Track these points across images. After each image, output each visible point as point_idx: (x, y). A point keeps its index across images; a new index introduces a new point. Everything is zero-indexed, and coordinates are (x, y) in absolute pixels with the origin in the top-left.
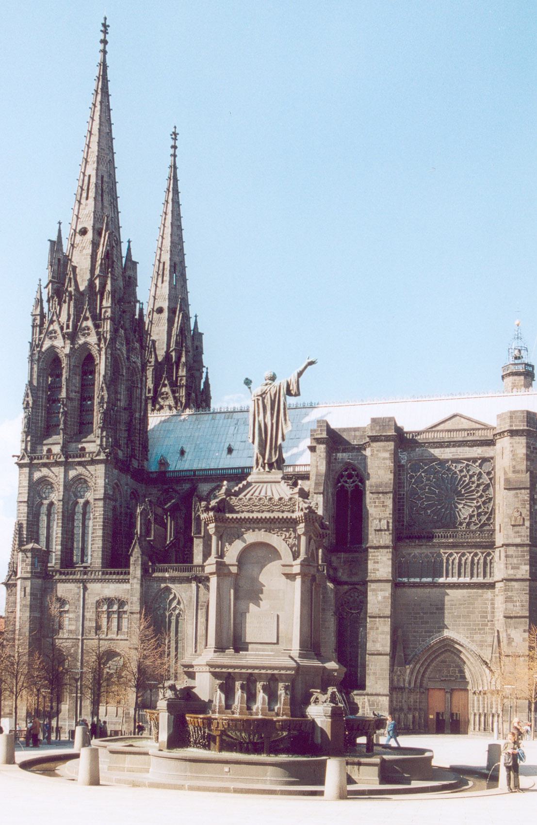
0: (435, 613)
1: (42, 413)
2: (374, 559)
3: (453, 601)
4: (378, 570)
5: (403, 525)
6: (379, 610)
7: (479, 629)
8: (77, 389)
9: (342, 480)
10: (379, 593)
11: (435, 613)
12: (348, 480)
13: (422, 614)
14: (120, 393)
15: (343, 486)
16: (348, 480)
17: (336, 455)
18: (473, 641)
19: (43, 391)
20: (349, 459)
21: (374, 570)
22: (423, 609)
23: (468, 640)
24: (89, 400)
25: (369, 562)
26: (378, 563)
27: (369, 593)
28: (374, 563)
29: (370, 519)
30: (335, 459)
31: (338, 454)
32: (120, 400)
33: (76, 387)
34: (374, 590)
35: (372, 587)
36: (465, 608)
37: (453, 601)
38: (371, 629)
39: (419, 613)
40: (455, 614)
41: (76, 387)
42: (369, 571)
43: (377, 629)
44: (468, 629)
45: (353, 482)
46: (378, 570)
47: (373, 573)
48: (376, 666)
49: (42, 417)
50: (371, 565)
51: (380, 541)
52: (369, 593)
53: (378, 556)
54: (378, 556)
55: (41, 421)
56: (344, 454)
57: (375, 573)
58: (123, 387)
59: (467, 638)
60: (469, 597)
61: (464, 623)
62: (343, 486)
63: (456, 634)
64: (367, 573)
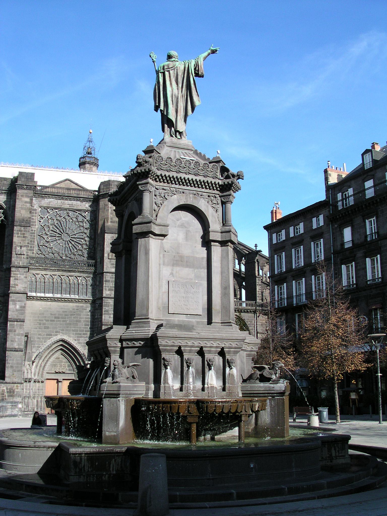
0: (54, 321)
2: (15, 277)
3: (66, 312)
4: (17, 285)
5: (33, 253)
6: (17, 316)
7: (84, 334)
10: (18, 303)
11: (54, 321)
13: (44, 321)
18: (79, 343)
21: (14, 284)
22: (46, 317)
23: (76, 342)
25: (11, 278)
26: (17, 279)
27: (10, 302)
28: (15, 279)
29: (14, 246)
34: (13, 301)
35: (12, 298)
36: (74, 318)
37: (66, 312)
38: (11, 331)
39: (43, 320)
40: (68, 322)
42: (11, 286)
43: (15, 331)
44: (76, 334)
46: (17, 285)
47: (14, 287)
48: (13, 360)
50: (12, 282)
51: (20, 263)
52: (10, 303)
53: (18, 274)
54: (18, 274)
57: (15, 287)
59: (75, 340)
60: (77, 310)
61: (74, 329)
63: (68, 337)
64: (9, 287)
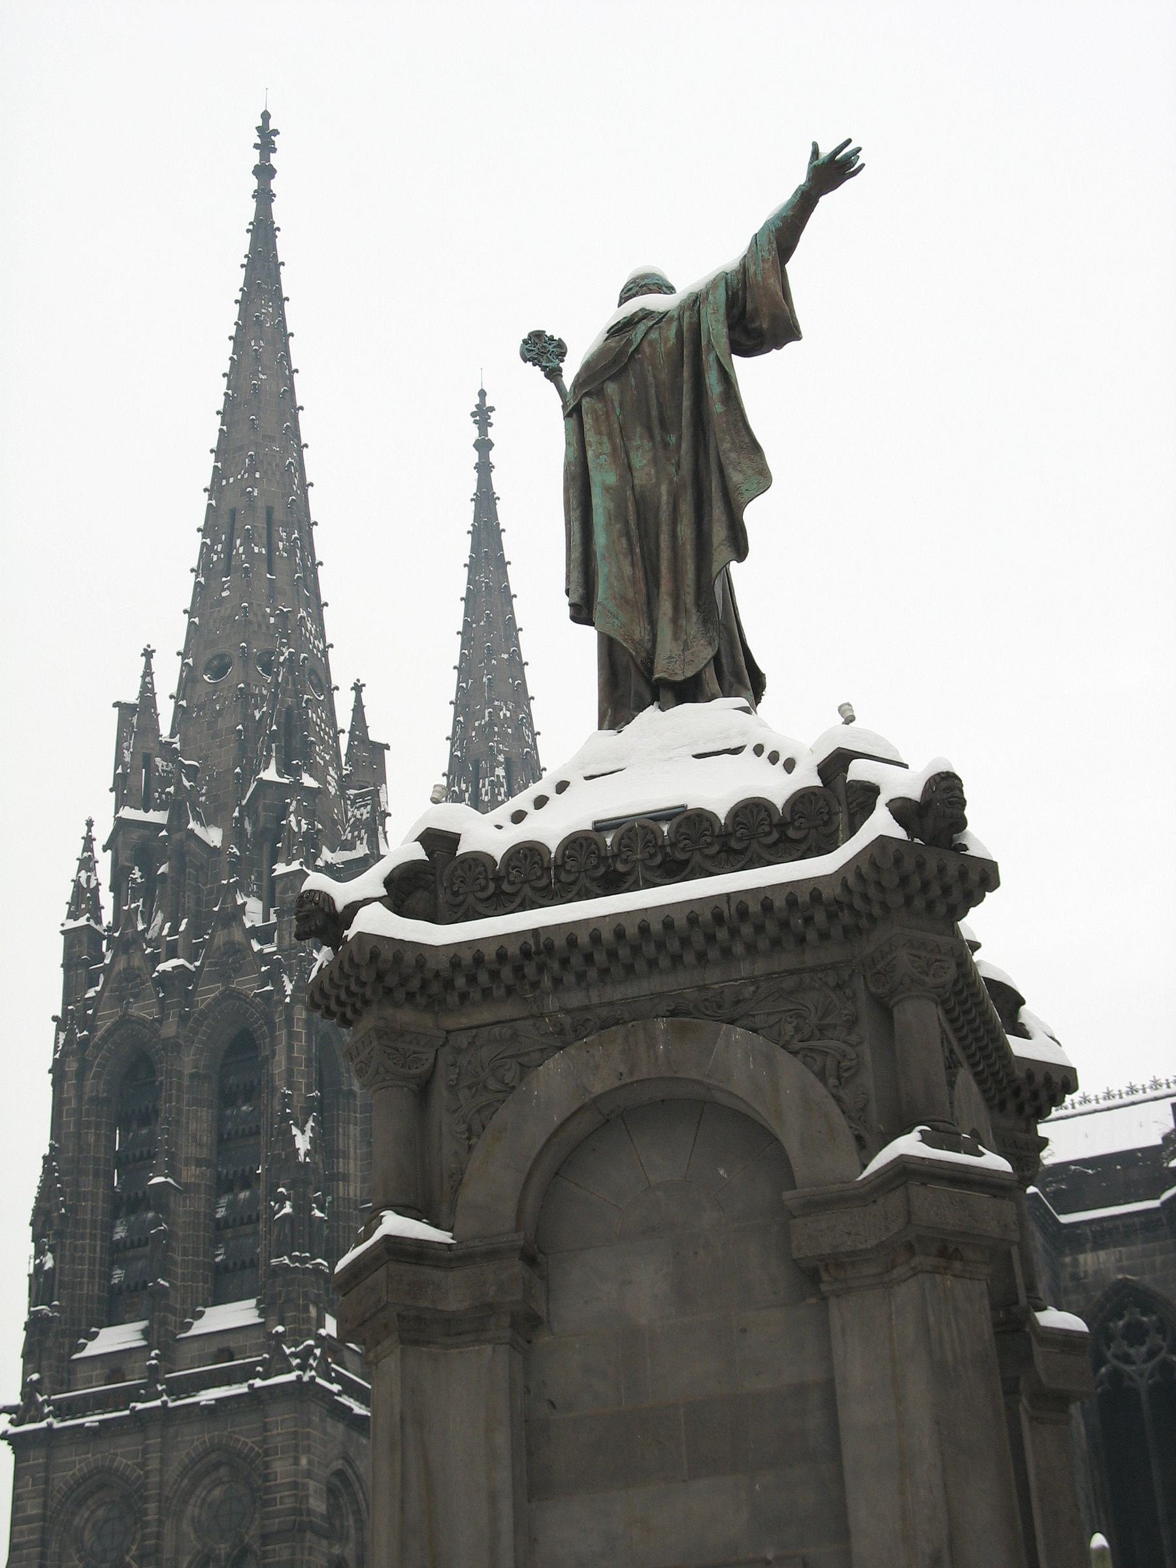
1: (93, 1249)
8: (204, 1153)
9: (1109, 1354)
12: (1132, 1351)
14: (346, 1156)
15: (1116, 1374)
16: (1132, 1351)
17: (1076, 1263)
19: (96, 1174)
20: (1121, 1270)
24: (243, 1189)
30: (1075, 1277)
31: (1081, 1258)
32: (345, 1178)
33: (200, 1145)
41: (200, 1145)
45: (1152, 1354)
49: (92, 1261)
55: (92, 1275)
56: (1102, 1254)
58: (354, 1131)
62: (1116, 1374)
